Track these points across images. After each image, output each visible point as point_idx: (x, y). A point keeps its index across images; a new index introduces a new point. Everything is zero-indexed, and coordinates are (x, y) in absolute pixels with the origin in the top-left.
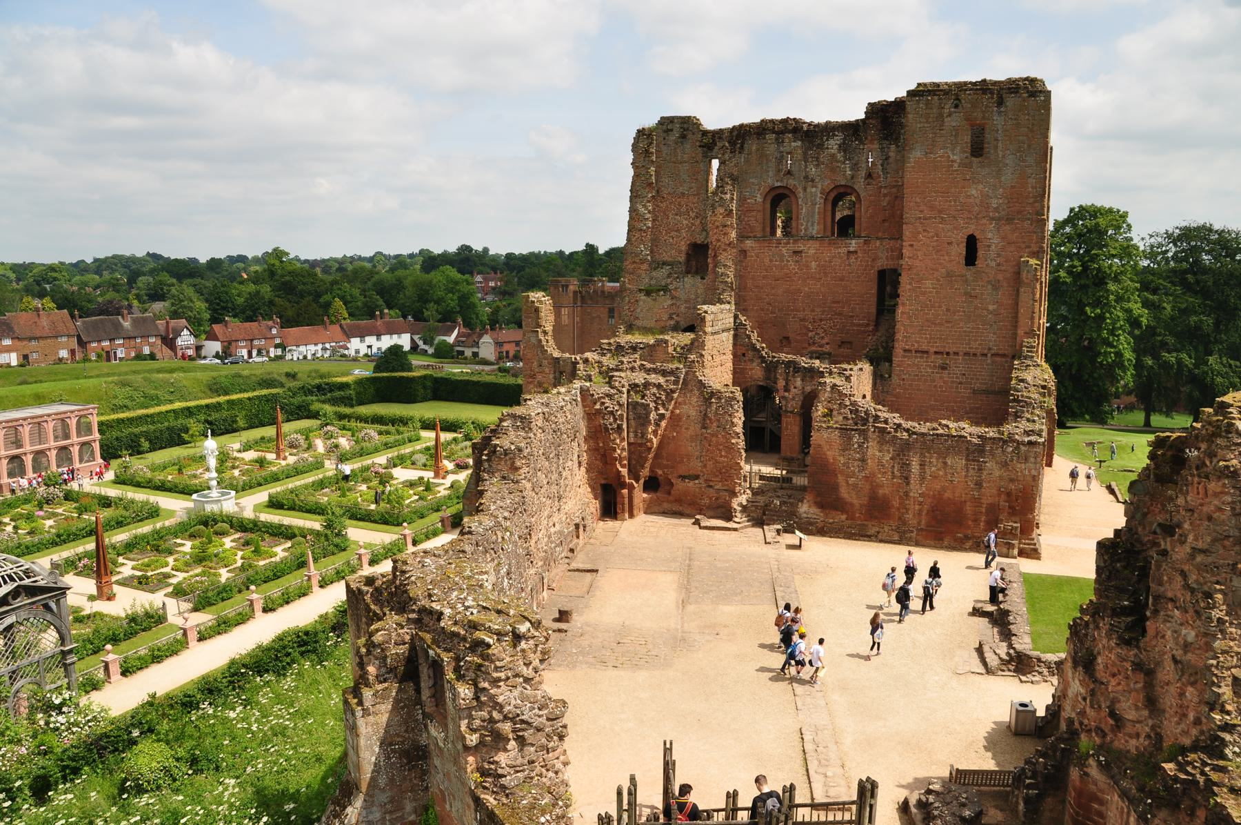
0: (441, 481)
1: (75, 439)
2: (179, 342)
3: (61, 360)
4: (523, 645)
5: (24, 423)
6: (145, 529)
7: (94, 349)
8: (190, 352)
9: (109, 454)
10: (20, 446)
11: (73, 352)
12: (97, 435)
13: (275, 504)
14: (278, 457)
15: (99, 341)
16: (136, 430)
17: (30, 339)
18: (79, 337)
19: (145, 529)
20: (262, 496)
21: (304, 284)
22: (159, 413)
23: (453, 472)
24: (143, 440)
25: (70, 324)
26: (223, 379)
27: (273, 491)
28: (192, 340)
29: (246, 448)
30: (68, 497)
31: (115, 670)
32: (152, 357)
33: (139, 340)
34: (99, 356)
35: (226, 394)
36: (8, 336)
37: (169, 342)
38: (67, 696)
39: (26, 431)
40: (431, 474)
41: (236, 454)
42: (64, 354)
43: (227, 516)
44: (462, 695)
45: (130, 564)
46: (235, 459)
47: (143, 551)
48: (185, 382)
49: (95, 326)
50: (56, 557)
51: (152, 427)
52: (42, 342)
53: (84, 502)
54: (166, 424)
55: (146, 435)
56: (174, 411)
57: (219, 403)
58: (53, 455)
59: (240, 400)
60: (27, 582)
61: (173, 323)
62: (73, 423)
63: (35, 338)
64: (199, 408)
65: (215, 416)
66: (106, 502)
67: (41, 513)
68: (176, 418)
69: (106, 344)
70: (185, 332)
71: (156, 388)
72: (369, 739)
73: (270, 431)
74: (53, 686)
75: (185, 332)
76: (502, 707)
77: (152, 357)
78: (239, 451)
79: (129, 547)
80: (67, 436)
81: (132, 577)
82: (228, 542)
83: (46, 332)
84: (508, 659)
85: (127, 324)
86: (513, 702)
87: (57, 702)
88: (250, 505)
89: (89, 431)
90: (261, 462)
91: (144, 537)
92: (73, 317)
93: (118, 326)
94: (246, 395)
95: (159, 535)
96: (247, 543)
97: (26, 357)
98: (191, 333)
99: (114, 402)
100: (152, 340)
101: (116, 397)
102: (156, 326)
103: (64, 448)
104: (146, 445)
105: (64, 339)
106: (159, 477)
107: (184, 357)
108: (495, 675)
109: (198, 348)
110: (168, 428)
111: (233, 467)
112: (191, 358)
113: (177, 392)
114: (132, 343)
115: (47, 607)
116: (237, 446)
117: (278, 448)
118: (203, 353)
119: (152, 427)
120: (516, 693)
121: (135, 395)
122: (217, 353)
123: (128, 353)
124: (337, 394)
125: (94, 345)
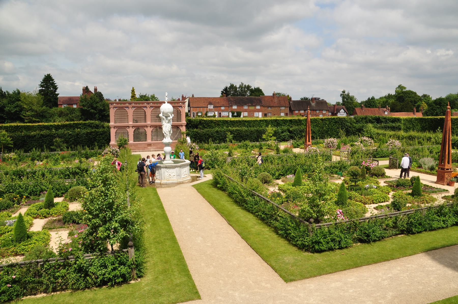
0: (446, 187)
15: (299, 110)
17: (268, 107)
18: (290, 108)
21: (409, 97)
33: (318, 112)
36: (259, 105)
40: (435, 178)
52: (273, 109)
57: (299, 120)
63: (270, 107)
70: (342, 110)
75: (342, 110)
98: (345, 111)
105: (283, 108)
110: (257, 131)
114: (315, 113)
124: (390, 124)
125: (297, 112)
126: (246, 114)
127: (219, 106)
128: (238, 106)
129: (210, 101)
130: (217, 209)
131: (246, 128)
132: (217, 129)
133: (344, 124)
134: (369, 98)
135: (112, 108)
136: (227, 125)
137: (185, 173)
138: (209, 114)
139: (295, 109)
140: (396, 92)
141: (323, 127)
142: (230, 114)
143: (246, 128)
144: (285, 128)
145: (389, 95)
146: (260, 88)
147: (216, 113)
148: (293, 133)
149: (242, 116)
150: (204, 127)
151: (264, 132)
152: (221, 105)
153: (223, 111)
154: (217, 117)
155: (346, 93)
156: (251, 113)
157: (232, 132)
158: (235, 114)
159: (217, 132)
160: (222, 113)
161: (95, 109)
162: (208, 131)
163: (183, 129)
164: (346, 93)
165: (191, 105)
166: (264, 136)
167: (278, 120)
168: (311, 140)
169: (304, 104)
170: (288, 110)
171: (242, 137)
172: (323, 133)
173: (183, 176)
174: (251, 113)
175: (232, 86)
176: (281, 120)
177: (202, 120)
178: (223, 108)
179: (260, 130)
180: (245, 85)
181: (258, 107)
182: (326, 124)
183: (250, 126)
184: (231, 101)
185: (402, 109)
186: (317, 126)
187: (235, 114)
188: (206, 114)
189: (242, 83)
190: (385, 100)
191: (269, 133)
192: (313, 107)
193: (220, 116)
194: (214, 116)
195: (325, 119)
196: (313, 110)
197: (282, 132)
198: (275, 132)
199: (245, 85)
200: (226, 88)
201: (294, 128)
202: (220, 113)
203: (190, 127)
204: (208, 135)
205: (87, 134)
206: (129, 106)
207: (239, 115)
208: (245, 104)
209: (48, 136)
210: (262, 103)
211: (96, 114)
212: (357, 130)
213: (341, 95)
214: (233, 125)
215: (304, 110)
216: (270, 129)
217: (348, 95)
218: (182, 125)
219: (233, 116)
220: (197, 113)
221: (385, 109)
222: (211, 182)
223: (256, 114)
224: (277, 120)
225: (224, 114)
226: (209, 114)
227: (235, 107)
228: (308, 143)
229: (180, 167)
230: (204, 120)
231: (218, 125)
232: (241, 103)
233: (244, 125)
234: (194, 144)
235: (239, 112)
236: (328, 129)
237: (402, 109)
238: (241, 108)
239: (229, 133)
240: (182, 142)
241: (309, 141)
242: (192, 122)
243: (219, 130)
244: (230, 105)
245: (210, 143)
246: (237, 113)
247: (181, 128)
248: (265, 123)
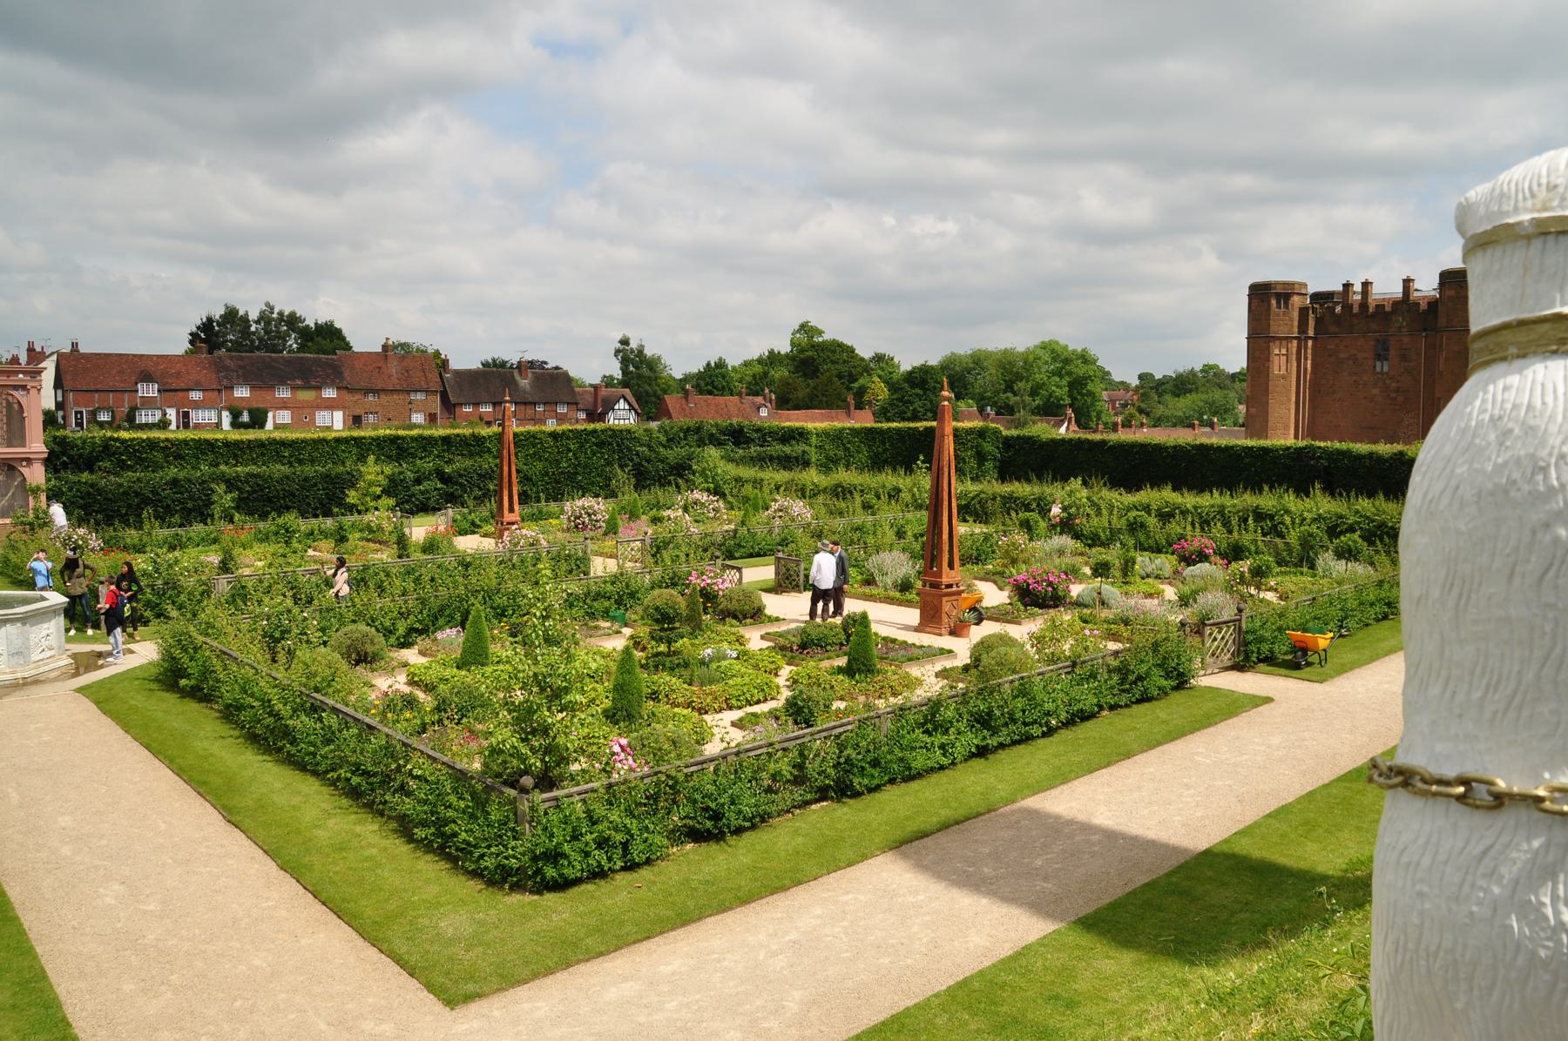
0: (946, 642)
15: (476, 405)
17: (367, 392)
23: (1000, 615)
33: (540, 409)
36: (331, 385)
40: (913, 616)
52: (384, 399)
57: (479, 440)
63: (376, 392)
70: (622, 404)
75: (622, 404)
83: (394, 383)
98: (632, 408)
104: (224, 498)
105: (420, 396)
110: (326, 477)
114: (530, 411)
125: (468, 409)
126: (285, 417)
127: (183, 386)
128: (253, 388)
129: (143, 368)
130: (179, 772)
131: (286, 469)
132: (173, 472)
133: (629, 449)
134: (708, 364)
136: (211, 457)
137: (44, 643)
138: (144, 417)
139: (461, 400)
140: (793, 344)
141: (558, 462)
142: (225, 414)
143: (286, 469)
144: (428, 465)
145: (771, 352)
146: (337, 325)
147: (172, 414)
148: (457, 483)
149: (269, 425)
150: (124, 466)
151: (351, 481)
153: (197, 405)
154: (173, 427)
155: (633, 345)
156: (303, 413)
157: (231, 484)
158: (245, 418)
159: (175, 482)
160: (193, 414)
162: (139, 480)
163: (36, 475)
164: (633, 345)
165: (67, 384)
166: (352, 497)
167: (403, 438)
168: (516, 507)
169: (495, 379)
170: (436, 404)
171: (270, 500)
172: (558, 482)
173: (35, 657)
174: (303, 413)
175: (231, 315)
176: (413, 439)
177: (111, 439)
178: (196, 395)
179: (338, 476)
180: (281, 314)
181: (330, 393)
183: (300, 462)
184: (226, 368)
185: (811, 400)
186: (537, 456)
187: (245, 418)
188: (130, 418)
189: (267, 304)
190: (758, 369)
191: (371, 484)
193: (186, 426)
194: (163, 425)
197: (418, 481)
198: (391, 479)
199: (281, 314)
200: (210, 320)
201: (460, 464)
202: (186, 415)
203: (65, 466)
204: (137, 494)
207: (258, 421)
208: (282, 382)
212: (672, 468)
213: (617, 352)
214: (235, 457)
215: (494, 404)
216: (374, 471)
217: (640, 352)
218: (29, 461)
219: (236, 424)
220: (93, 414)
221: (759, 399)
222: (155, 671)
223: (322, 418)
224: (398, 438)
225: (198, 416)
226: (144, 417)
227: (242, 393)
228: (508, 517)
229: (25, 619)
230: (123, 441)
231: (179, 457)
232: (265, 377)
233: (279, 458)
234: (81, 531)
235: (258, 409)
236: (576, 467)
237: (811, 400)
239: (220, 489)
240: (31, 524)
241: (511, 510)
242: (73, 445)
243: (181, 475)
244: (225, 382)
245: (147, 527)
246: (250, 412)
247: (25, 471)
248: (355, 451)
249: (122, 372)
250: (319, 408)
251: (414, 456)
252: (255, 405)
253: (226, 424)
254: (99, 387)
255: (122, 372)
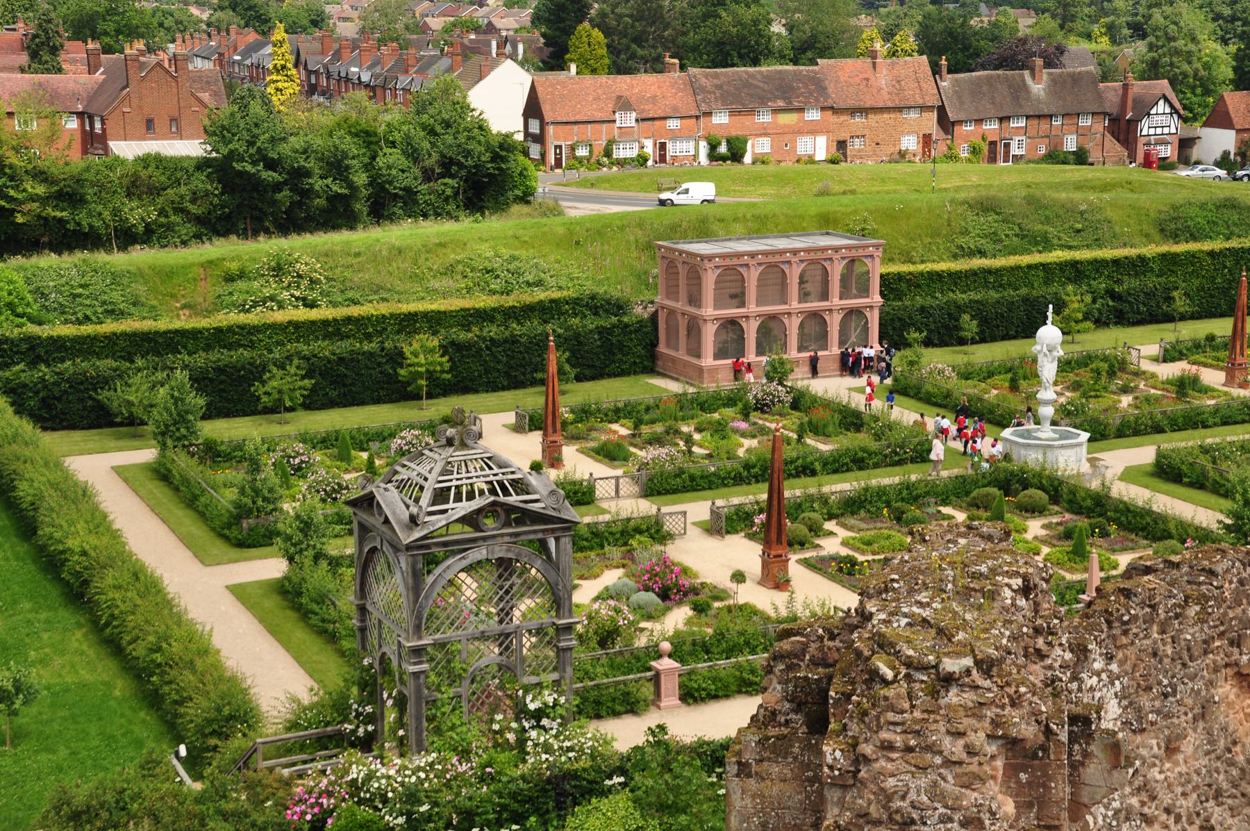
1: (836, 301)
2: (1145, 128)
3: (902, 155)
4: (952, 697)
5: (752, 262)
6: (887, 479)
7: (966, 138)
8: (1167, 152)
9: (893, 335)
10: (742, 304)
11: (927, 140)
12: (877, 299)
13: (1167, 472)
14: (1230, 381)
15: (979, 121)
16: (961, 297)
17: (853, 111)
18: (942, 111)
19: (887, 479)
20: (1144, 454)
22: (1014, 269)
24: (966, 317)
25: (929, 85)
26: (1193, 211)
27: (1166, 446)
28: (1173, 126)
29: (1168, 356)
30: (799, 402)
31: (670, 687)
32: (1080, 157)
33: (1057, 123)
34: (975, 151)
35: (1194, 238)
37: (1123, 129)
38: (550, 700)
39: (752, 277)
41: (1146, 366)
42: (910, 143)
43: (1051, 479)
44: (829, 759)
45: (843, 533)
46: (1138, 374)
47: (875, 516)
48: (1109, 213)
49: (976, 86)
50: (719, 503)
51: (993, 295)
53: (820, 415)
54: (1024, 291)
55: (978, 310)
56: (1044, 266)
57: (1142, 259)
58: (793, 325)
59: (1191, 256)
60: (514, 499)
61: (1139, 87)
62: (837, 270)
64: (1098, 265)
65: (1129, 284)
66: (852, 420)
67: (743, 425)
68: (1047, 282)
69: (992, 127)
70: (1162, 107)
71: (1047, 220)
72: (747, 819)
73: (1222, 327)
74: (534, 680)
75: (1162, 107)
76: (889, 798)
77: (1080, 157)
78: (1156, 360)
79: (851, 506)
80: (825, 296)
81: (833, 558)
82: (1035, 527)
83: (884, 100)
84: (917, 714)
85: (1038, 87)
86: (912, 796)
87: (532, 707)
88: (1120, 470)
89: (864, 291)
90: (1184, 386)
91: (881, 492)
92: (936, 70)
93: (1020, 90)
94: (1207, 246)
95: (912, 494)
96: (1068, 535)
97: (842, 145)
98: (1174, 110)
99: (962, 241)
100: (1086, 122)
101: (965, 232)
102: (1099, 96)
103: (817, 317)
104: (970, 325)
105: (913, 115)
106: (967, 390)
107: (1148, 163)
108: (885, 735)
109: (1186, 144)
110: (1026, 300)
111: (1125, 390)
112: (1165, 164)
113: (1087, 227)
114: (1044, 125)
115: (543, 545)
116: (1154, 349)
117: (1232, 360)
118: (1195, 153)
119: (993, 295)
120: (923, 782)
121: (1003, 230)
122: (1226, 154)
123: (1032, 148)
125: (969, 128)
127: (660, 113)
128: (732, 113)
135: (710, 271)
138: (621, 153)
139: (962, 117)
142: (703, 146)
148: (1127, 301)
149: (748, 159)
152: (669, 112)
158: (723, 149)
160: (669, 146)
161: (271, 165)
170: (930, 122)
174: (784, 136)
178: (673, 124)
181: (813, 115)
182: (1225, 267)
184: (703, 90)
187: (723, 149)
188: (608, 153)
192: (1038, 100)
193: (663, 159)
195: (1221, 251)
196: (1039, 117)
202: (663, 146)
204: (900, 319)
205: (601, 331)
206: (752, 262)
207: (736, 156)
208: (763, 102)
209: (506, 341)
210: (827, 96)
211: (277, 187)
215: (1001, 120)
219: (713, 156)
220: (573, 148)
222: (1149, 469)
225: (673, 149)
227: (721, 119)
233: (986, 285)
235: (737, 138)
238: (746, 120)
244: (704, 108)
246: (728, 142)
247: (868, 315)
248: (1041, 274)
249: (597, 99)
250: (801, 132)
251: (1088, 277)
252: (734, 133)
253: (703, 159)
254: (578, 118)
255: (597, 99)
